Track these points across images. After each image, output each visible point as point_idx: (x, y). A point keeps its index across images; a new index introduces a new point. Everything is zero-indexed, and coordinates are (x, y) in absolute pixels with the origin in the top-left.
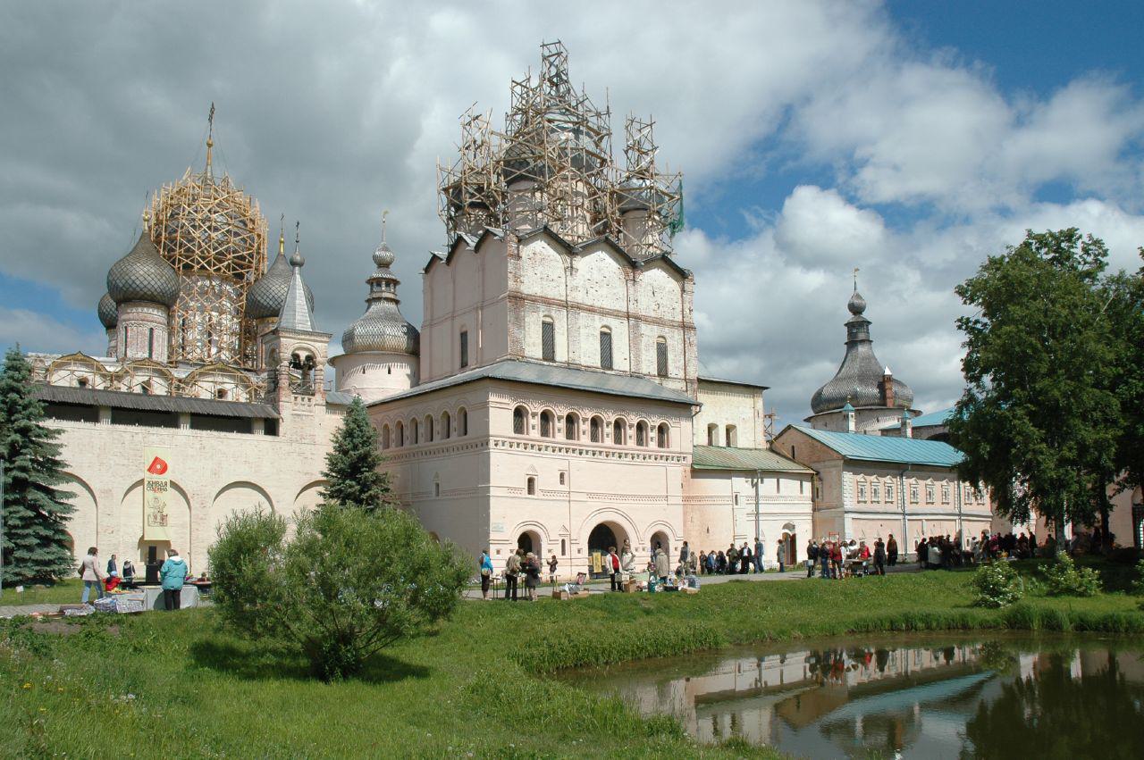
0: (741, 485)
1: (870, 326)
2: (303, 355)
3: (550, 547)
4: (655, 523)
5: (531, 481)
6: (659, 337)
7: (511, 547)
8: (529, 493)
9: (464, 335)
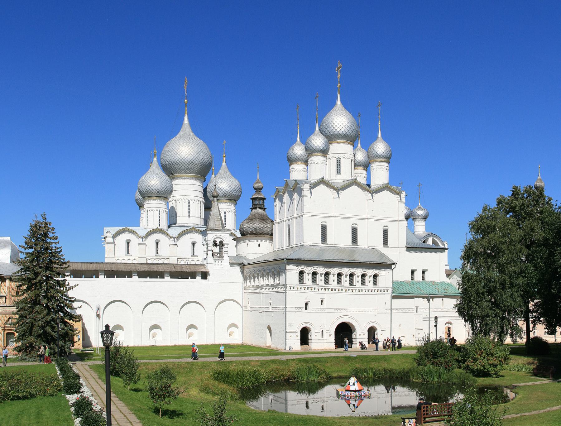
0: (421, 303)
2: (218, 241)
3: (316, 334)
4: (370, 322)
5: (307, 304)
7: (297, 334)
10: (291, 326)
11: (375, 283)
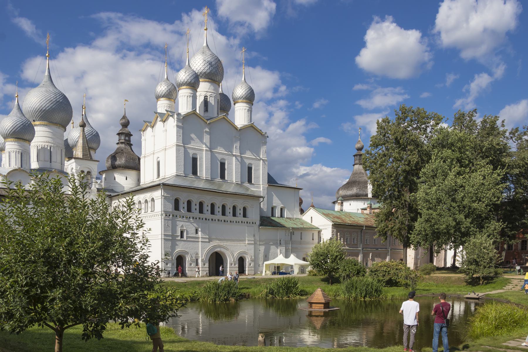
5: (182, 233)
9: (158, 163)
11: (245, 216)
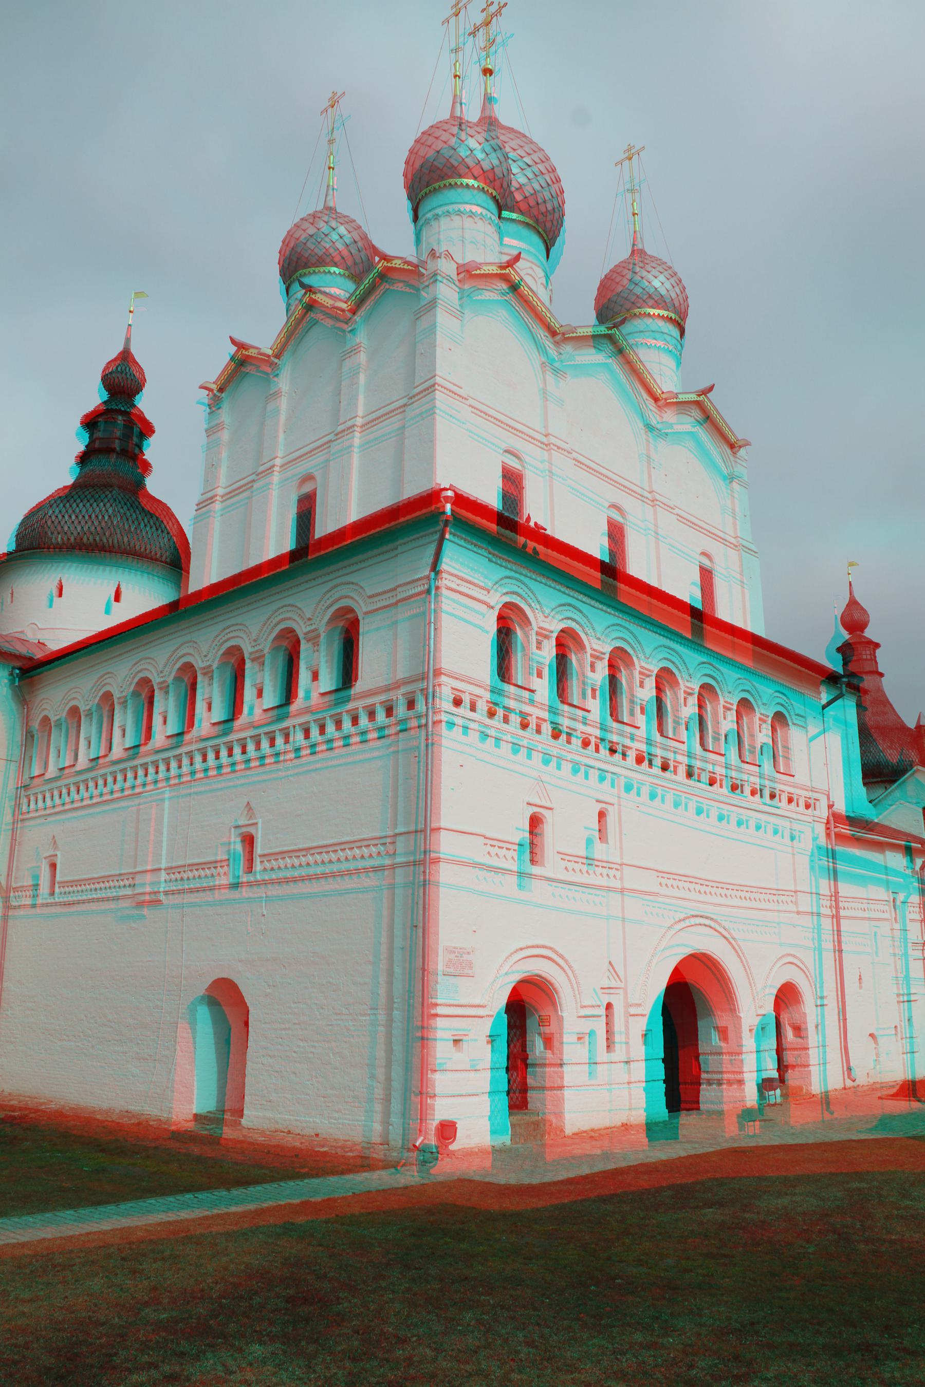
1: (878, 652)
6: (703, 554)
8: (533, 861)
10: (462, 968)
